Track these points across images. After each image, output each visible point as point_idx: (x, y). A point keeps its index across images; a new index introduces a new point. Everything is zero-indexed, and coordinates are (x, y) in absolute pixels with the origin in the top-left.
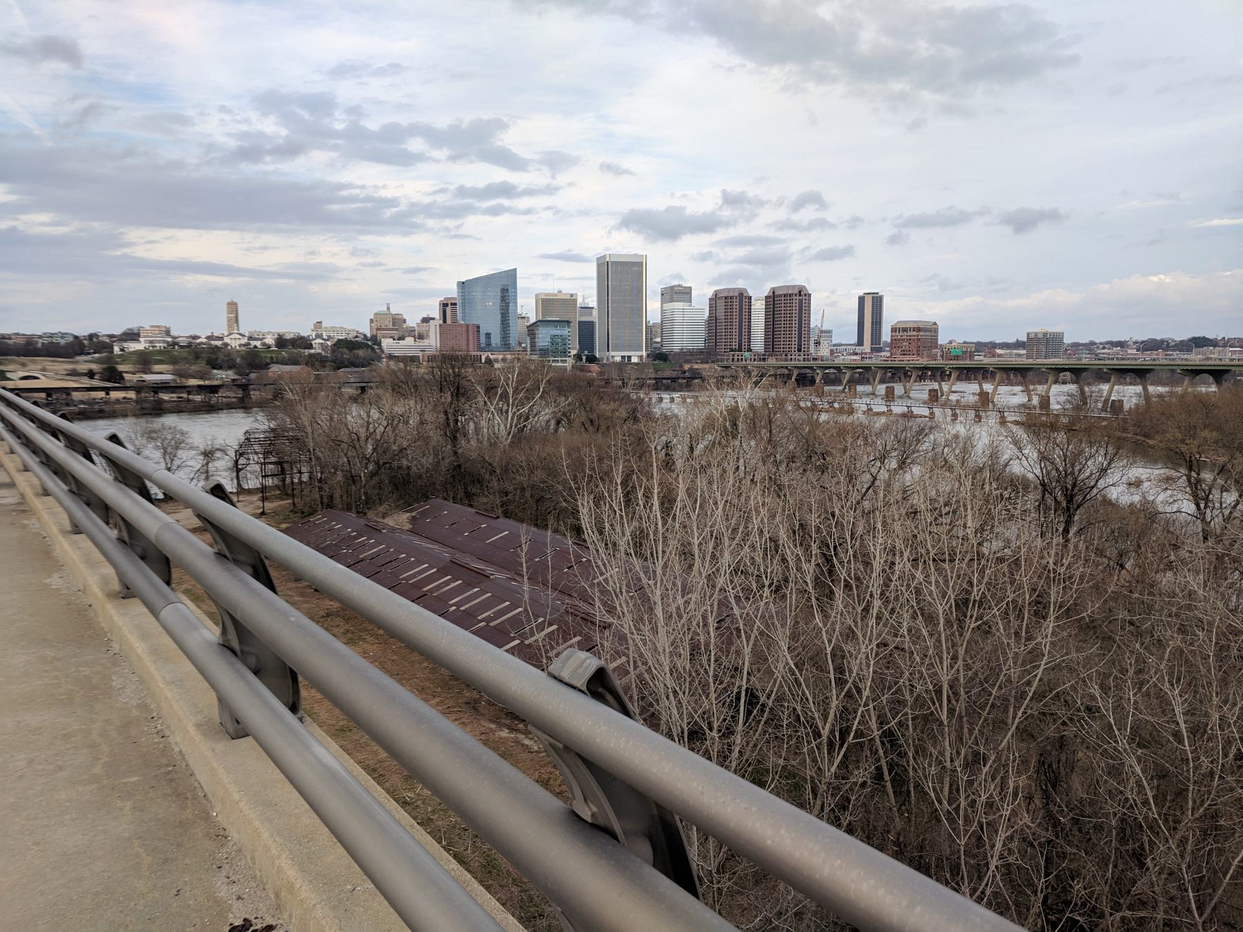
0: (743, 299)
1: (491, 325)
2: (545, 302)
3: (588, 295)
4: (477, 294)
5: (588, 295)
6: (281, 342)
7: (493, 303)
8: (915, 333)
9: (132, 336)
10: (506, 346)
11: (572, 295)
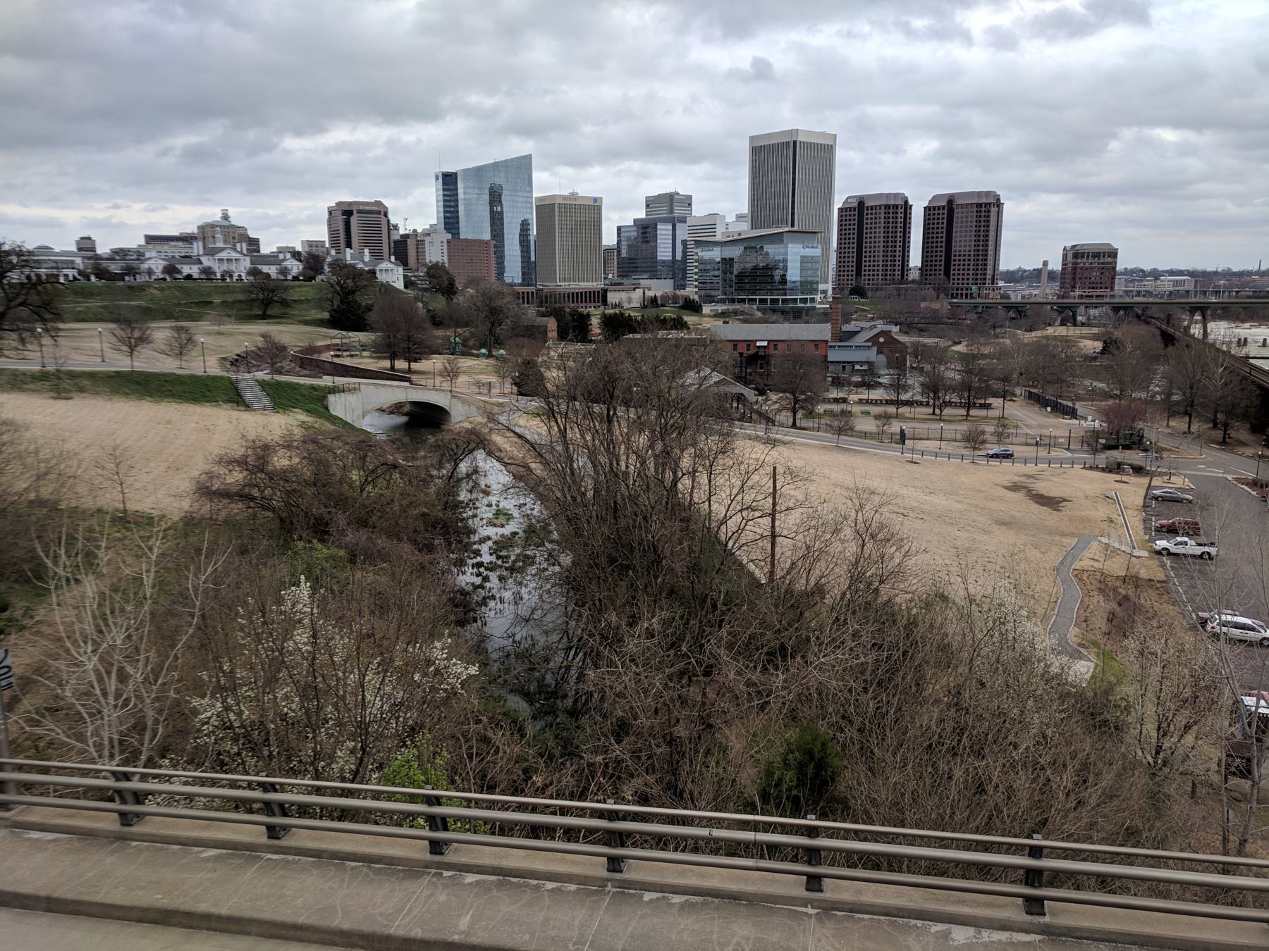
0: (898, 210)
8: (1109, 259)
11: (595, 200)
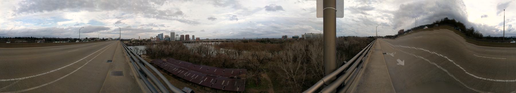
1: (161, 38)
2: (166, 36)
3: (170, 35)
4: (160, 35)
5: (170, 35)
6: (143, 40)
7: (161, 36)
9: (132, 39)
10: (162, 40)
